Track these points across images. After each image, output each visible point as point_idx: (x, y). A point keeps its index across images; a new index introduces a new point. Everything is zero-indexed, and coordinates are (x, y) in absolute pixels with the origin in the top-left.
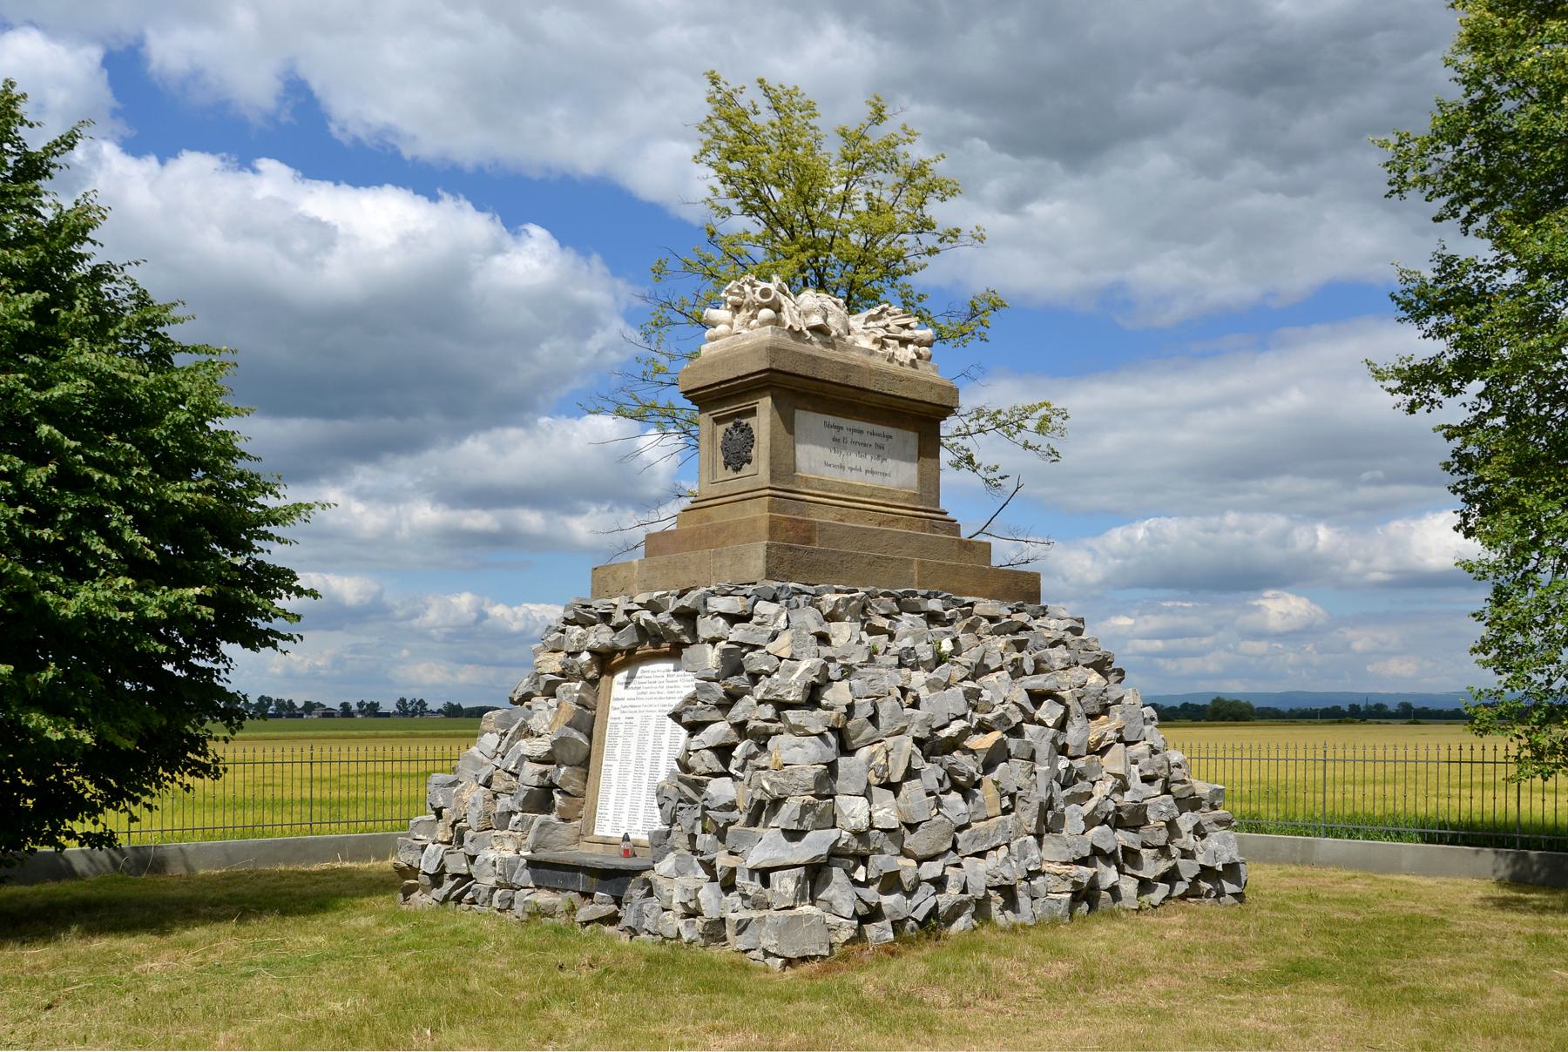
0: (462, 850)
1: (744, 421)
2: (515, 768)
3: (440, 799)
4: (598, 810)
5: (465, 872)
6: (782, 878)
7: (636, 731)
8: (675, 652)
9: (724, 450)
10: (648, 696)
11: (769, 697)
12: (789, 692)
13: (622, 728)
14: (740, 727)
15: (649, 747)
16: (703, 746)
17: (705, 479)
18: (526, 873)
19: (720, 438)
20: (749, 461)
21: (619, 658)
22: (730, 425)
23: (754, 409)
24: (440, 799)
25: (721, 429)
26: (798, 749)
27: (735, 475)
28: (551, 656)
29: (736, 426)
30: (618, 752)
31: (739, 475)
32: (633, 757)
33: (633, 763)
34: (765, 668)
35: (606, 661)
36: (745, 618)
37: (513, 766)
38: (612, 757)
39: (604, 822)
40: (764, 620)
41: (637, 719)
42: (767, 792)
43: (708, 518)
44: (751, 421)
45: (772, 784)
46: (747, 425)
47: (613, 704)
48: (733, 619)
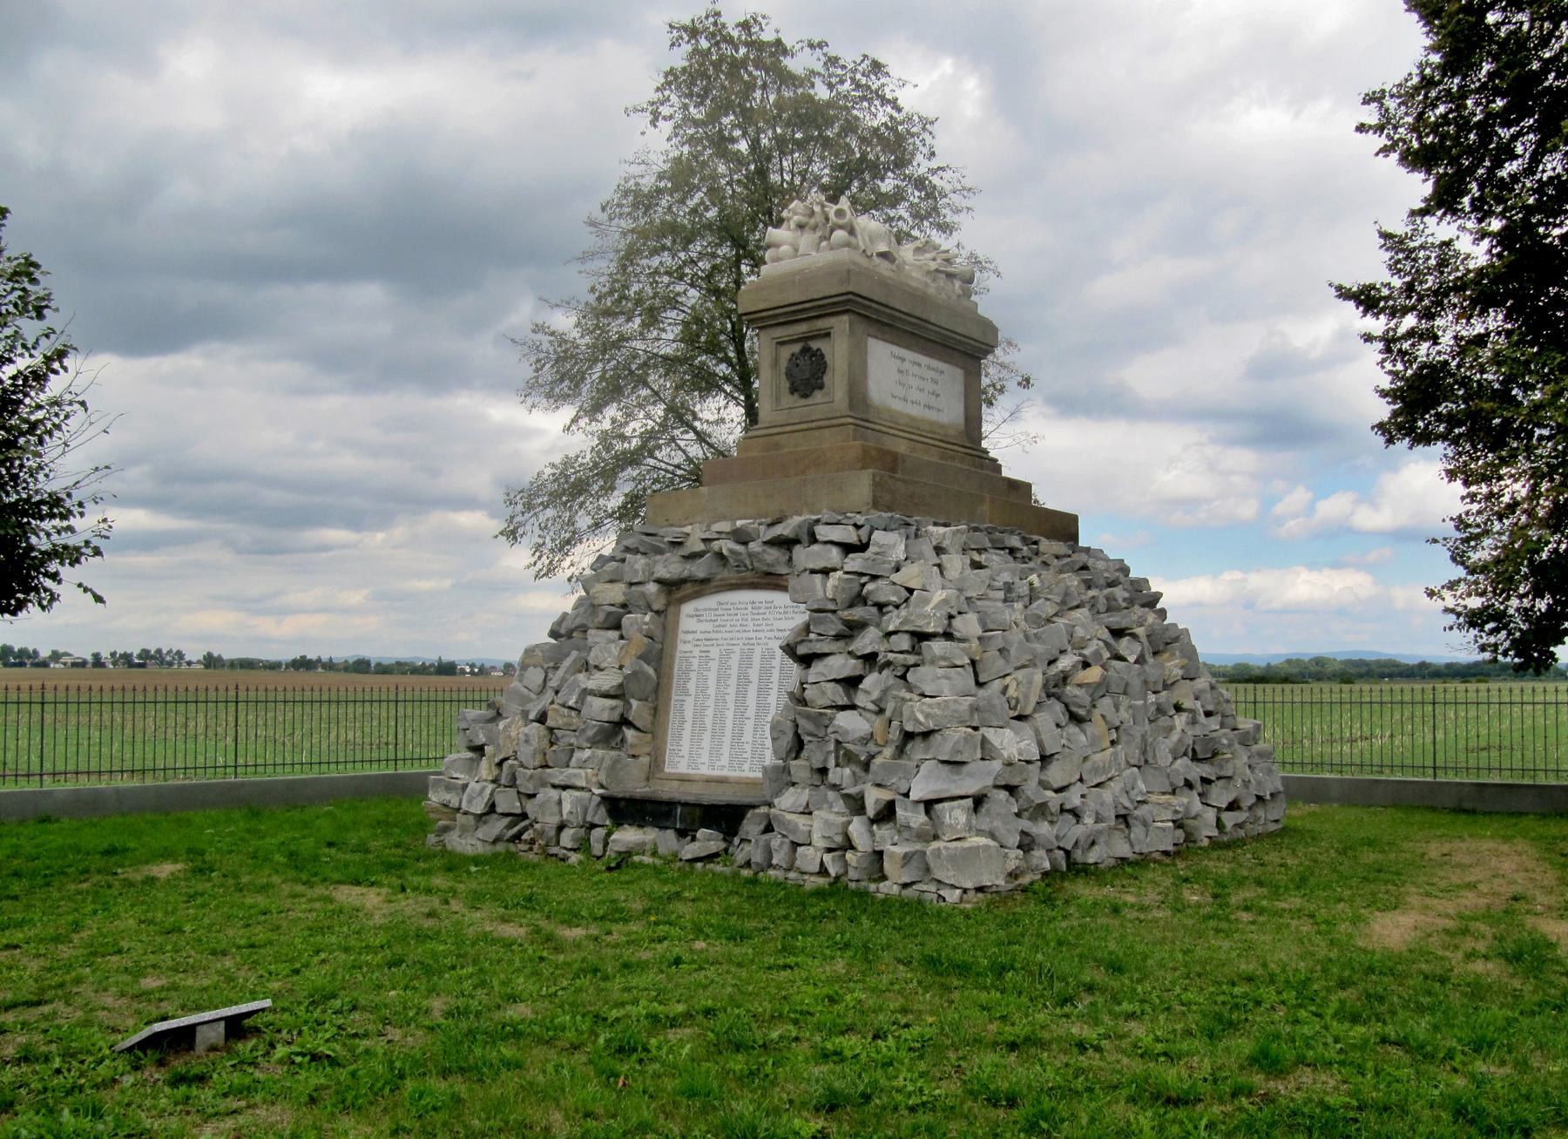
1: (814, 345)
3: (481, 736)
5: (518, 811)
6: (952, 809)
7: (714, 665)
8: (771, 581)
9: (789, 374)
10: (728, 628)
11: (906, 628)
13: (695, 662)
14: (870, 659)
15: (733, 681)
19: (784, 364)
20: (821, 387)
24: (481, 736)
27: (803, 402)
28: (609, 586)
29: (806, 350)
30: (692, 686)
31: (810, 401)
32: (711, 691)
33: (713, 697)
34: (894, 599)
35: (676, 590)
36: (862, 547)
39: (677, 759)
41: (715, 652)
42: (920, 723)
45: (927, 716)
46: (818, 350)
47: (681, 636)
48: (848, 549)
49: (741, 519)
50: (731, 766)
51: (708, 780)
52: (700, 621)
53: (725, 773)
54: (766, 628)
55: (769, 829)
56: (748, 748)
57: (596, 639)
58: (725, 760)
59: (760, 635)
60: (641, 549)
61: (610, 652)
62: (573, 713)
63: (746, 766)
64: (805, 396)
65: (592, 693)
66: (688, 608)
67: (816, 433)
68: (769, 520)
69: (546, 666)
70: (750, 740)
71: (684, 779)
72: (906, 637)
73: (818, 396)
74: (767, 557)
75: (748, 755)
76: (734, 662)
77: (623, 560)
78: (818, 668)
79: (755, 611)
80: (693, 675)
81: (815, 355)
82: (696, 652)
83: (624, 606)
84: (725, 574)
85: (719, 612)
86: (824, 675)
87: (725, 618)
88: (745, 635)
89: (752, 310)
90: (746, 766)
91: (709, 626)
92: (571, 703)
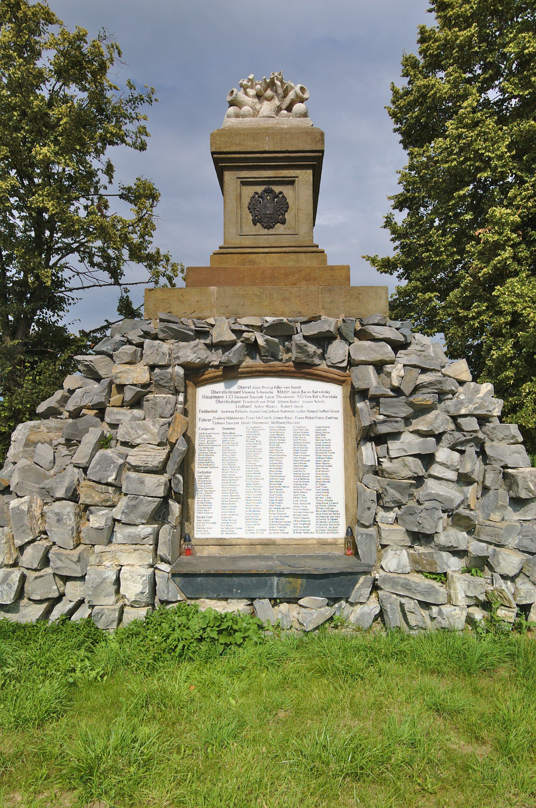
0: (49, 570)
1: (277, 189)
2: (115, 479)
4: (196, 514)
7: (242, 441)
9: (252, 208)
12: (494, 409)
13: (219, 439)
16: (405, 454)
17: (233, 231)
18: (173, 586)
19: (246, 201)
20: (283, 222)
21: (210, 373)
22: (260, 189)
23: (294, 181)
25: (249, 191)
26: (516, 455)
27: (266, 231)
28: (128, 367)
29: (269, 191)
30: (217, 459)
31: (271, 231)
32: (241, 462)
37: (114, 477)
38: (209, 463)
40: (423, 349)
41: (240, 429)
43: (253, 262)
44: (287, 191)
46: (281, 193)
47: (199, 415)
49: (274, 315)
50: (272, 529)
51: (252, 544)
52: (219, 402)
53: (266, 535)
54: (296, 409)
55: (375, 588)
56: (290, 513)
57: (118, 417)
58: (265, 524)
59: (288, 415)
60: (161, 336)
61: (146, 430)
62: (111, 489)
63: (290, 529)
64: (269, 227)
65: (136, 469)
66: (203, 391)
67: (292, 256)
68: (305, 319)
69: (55, 443)
70: (291, 506)
71: (221, 543)
72: (475, 420)
73: (279, 228)
74: (309, 349)
75: (291, 519)
76: (264, 437)
77: (141, 345)
78: (394, 446)
79: (280, 395)
80: (218, 450)
81: (277, 196)
82: (219, 429)
83: (144, 386)
84: (257, 363)
85: (241, 395)
86: (405, 451)
87: (249, 399)
88: (272, 415)
89: (225, 150)
90: (290, 529)
91: (232, 407)
92: (110, 480)
